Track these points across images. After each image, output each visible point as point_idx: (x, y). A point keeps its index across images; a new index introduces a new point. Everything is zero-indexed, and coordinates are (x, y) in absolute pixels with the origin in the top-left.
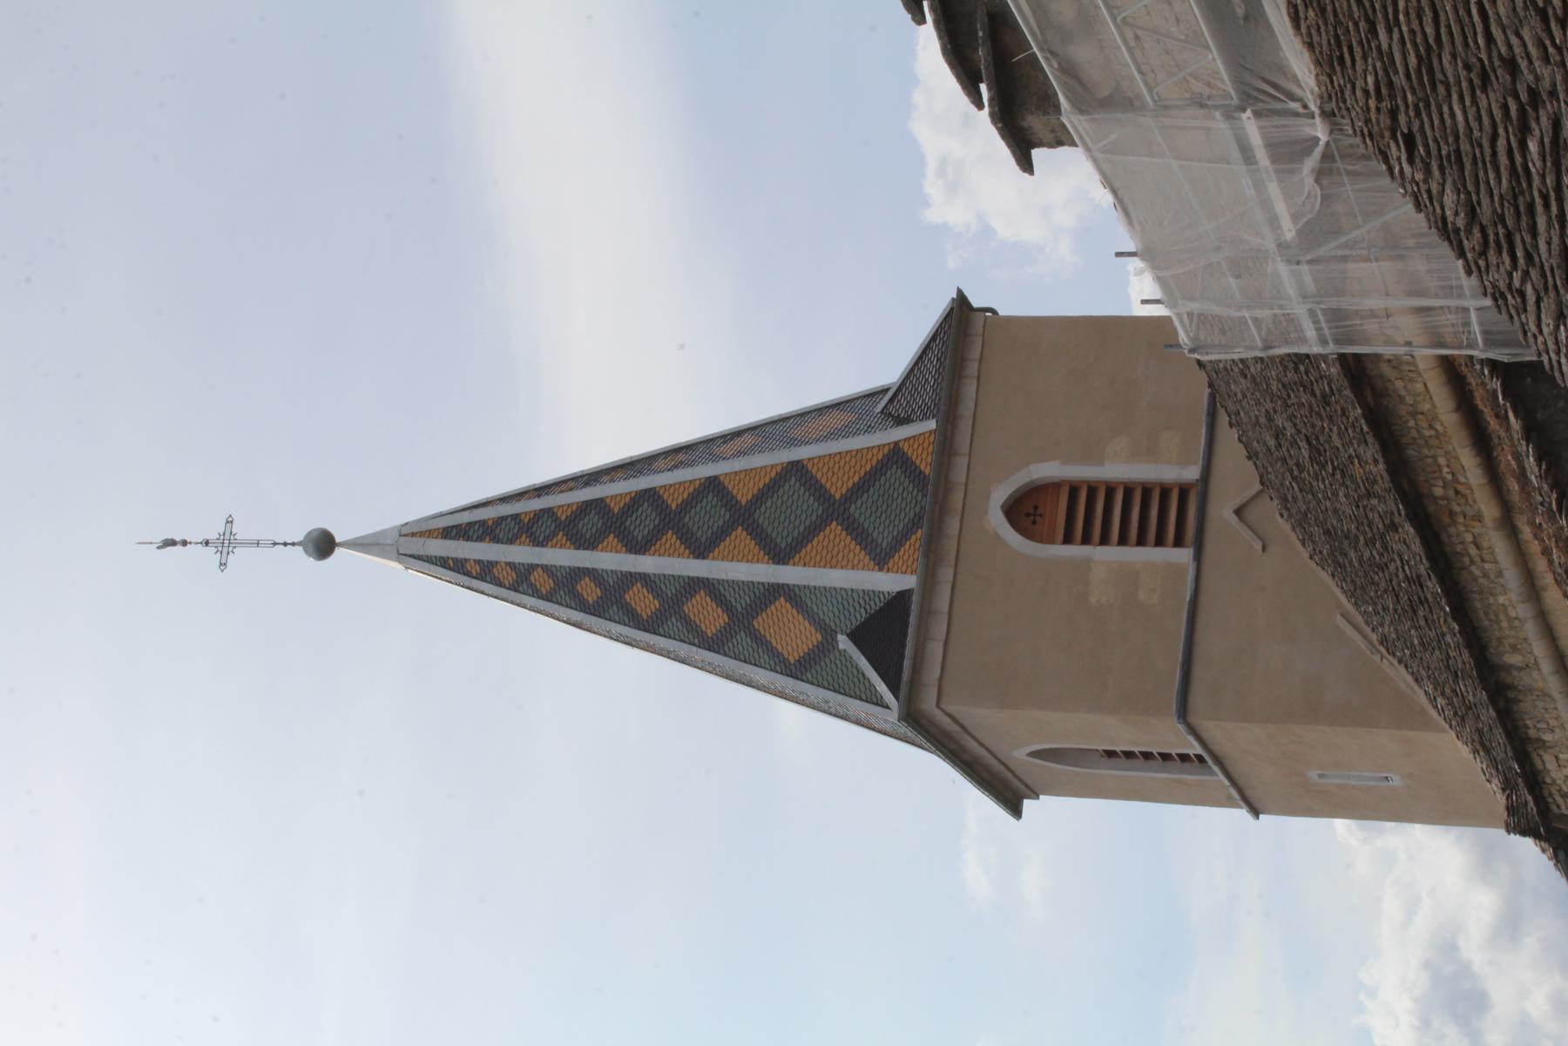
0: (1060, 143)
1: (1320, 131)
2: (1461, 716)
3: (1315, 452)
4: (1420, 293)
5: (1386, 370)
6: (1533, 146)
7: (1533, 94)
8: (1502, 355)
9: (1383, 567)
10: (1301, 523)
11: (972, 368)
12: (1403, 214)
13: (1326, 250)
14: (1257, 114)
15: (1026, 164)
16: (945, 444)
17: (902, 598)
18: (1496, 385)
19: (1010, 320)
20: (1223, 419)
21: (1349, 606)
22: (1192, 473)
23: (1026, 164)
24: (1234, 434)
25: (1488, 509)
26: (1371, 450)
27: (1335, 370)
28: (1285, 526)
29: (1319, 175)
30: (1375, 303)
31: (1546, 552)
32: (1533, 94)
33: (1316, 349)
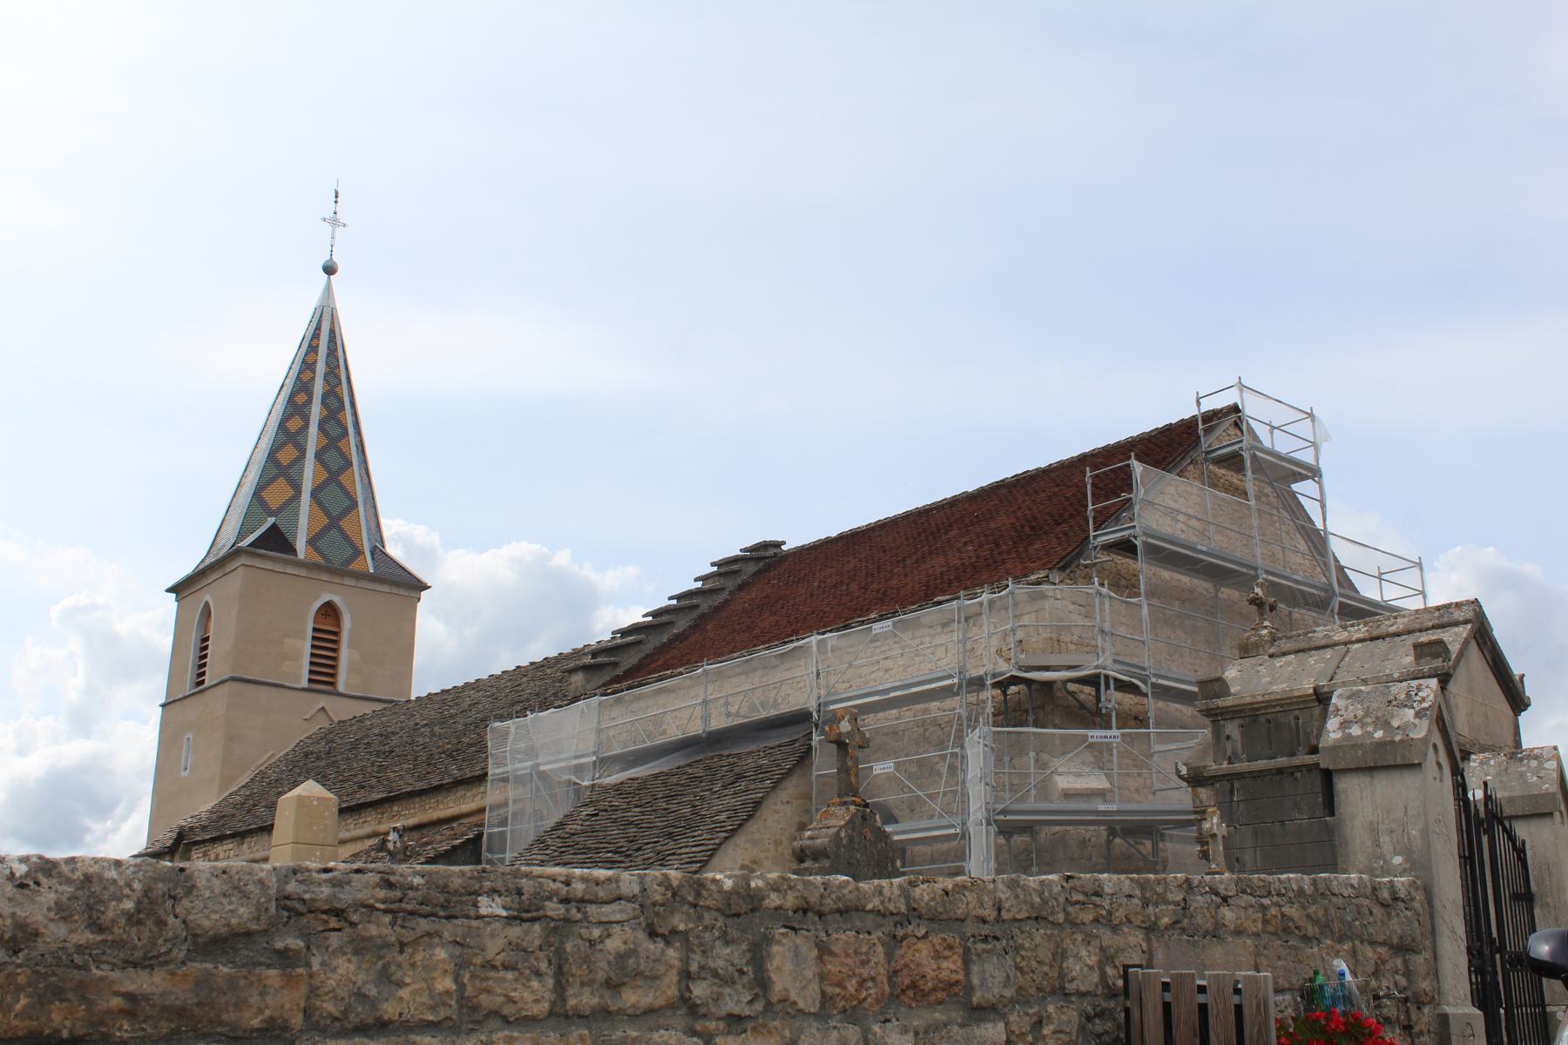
17: (294, 551)
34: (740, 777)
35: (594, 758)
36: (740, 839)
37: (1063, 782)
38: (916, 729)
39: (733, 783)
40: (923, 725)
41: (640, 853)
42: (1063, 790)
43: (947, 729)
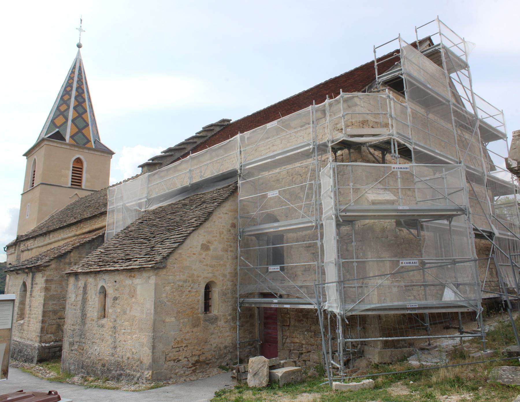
1: (143, 210)
2: (40, 228)
3: (88, 207)
6: (142, 240)
7: (150, 240)
8: (106, 235)
9: (67, 216)
10: (74, 204)
11: (102, 154)
12: (129, 222)
14: (146, 201)
16: (90, 149)
18: (101, 234)
19: (110, 161)
22: (83, 187)
25: (78, 233)
26: (89, 215)
28: (74, 201)
30: (115, 217)
32: (150, 240)
33: (108, 207)
34: (204, 202)
35: (146, 200)
37: (372, 196)
38: (288, 177)
39: (200, 205)
40: (292, 175)
41: (154, 239)
42: (372, 200)
43: (305, 176)
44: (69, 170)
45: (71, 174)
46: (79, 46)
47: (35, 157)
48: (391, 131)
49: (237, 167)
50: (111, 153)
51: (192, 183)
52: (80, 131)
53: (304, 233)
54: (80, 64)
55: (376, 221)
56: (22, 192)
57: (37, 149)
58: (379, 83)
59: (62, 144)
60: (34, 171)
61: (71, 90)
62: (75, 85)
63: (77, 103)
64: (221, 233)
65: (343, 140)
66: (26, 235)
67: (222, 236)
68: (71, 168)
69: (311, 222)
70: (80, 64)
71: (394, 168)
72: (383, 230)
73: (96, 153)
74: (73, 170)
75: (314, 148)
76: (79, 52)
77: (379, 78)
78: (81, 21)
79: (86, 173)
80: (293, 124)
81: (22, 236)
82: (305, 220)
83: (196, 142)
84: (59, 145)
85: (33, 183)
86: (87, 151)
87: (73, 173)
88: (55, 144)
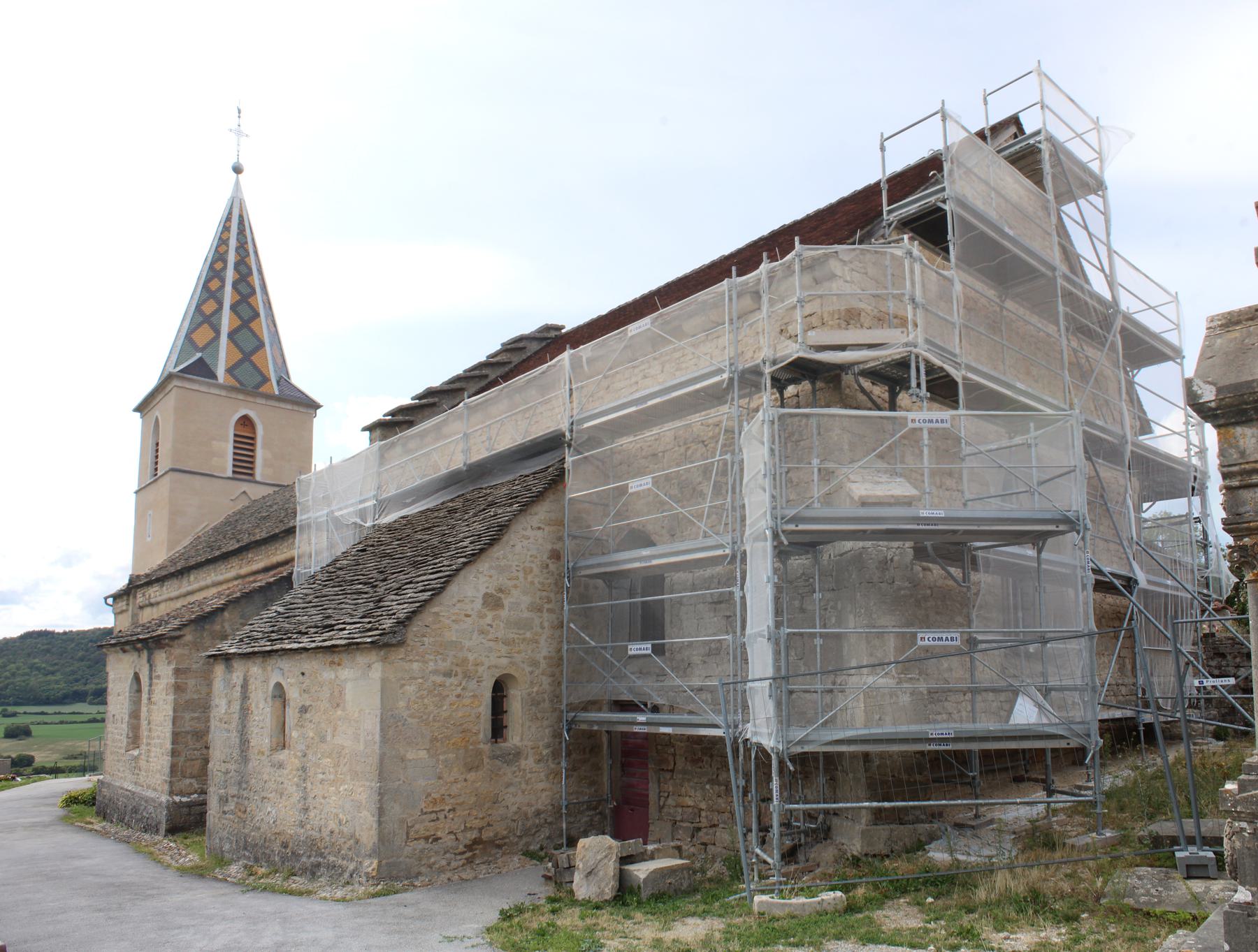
0: (371, 440)
1: (369, 524)
2: (172, 561)
3: (264, 518)
4: (316, 554)
5: (290, 541)
7: (376, 586)
8: (294, 576)
9: (224, 538)
10: (240, 512)
11: (296, 408)
12: (341, 548)
13: (331, 526)
15: (365, 429)
18: (285, 574)
19: (312, 422)
20: (277, 489)
21: (211, 526)
22: (258, 477)
23: (365, 429)
24: (271, 492)
25: (243, 571)
26: (264, 535)
27: (291, 525)
28: (239, 507)
29: (355, 523)
30: (313, 541)
31: (229, 588)
32: (376, 586)
33: (298, 518)
34: (491, 505)
36: (484, 565)
37: (860, 489)
38: (677, 448)
39: (484, 510)
40: (685, 444)
42: (861, 497)
43: (712, 445)
44: (227, 441)
45: (230, 450)
46: (237, 170)
47: (156, 413)
48: (911, 336)
49: (564, 426)
50: (314, 406)
51: (468, 462)
52: (247, 357)
53: (709, 572)
54: (241, 210)
55: (869, 544)
56: (136, 488)
57: (161, 396)
58: (890, 225)
59: (210, 385)
60: (157, 444)
61: (225, 268)
62: (232, 258)
63: (238, 298)
64: (528, 571)
65: (799, 359)
66: (147, 575)
67: (530, 578)
68: (231, 438)
69: (721, 546)
70: (241, 210)
71: (913, 421)
72: (884, 564)
73: (282, 405)
74: (235, 441)
75: (731, 380)
76: (237, 184)
77: (890, 212)
78: (239, 112)
79: (265, 446)
80: (688, 326)
81: (138, 577)
82: (709, 542)
83: (486, 376)
84: (203, 389)
85: (156, 469)
86: (263, 401)
87: (235, 448)
88: (196, 387)
